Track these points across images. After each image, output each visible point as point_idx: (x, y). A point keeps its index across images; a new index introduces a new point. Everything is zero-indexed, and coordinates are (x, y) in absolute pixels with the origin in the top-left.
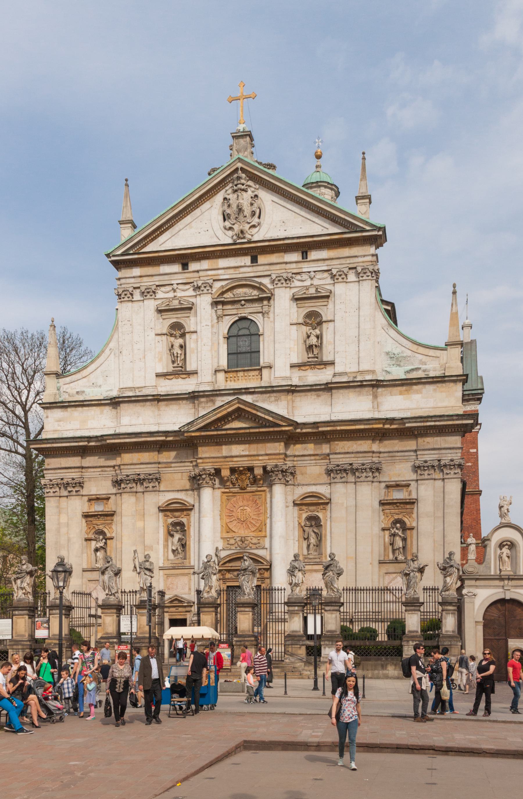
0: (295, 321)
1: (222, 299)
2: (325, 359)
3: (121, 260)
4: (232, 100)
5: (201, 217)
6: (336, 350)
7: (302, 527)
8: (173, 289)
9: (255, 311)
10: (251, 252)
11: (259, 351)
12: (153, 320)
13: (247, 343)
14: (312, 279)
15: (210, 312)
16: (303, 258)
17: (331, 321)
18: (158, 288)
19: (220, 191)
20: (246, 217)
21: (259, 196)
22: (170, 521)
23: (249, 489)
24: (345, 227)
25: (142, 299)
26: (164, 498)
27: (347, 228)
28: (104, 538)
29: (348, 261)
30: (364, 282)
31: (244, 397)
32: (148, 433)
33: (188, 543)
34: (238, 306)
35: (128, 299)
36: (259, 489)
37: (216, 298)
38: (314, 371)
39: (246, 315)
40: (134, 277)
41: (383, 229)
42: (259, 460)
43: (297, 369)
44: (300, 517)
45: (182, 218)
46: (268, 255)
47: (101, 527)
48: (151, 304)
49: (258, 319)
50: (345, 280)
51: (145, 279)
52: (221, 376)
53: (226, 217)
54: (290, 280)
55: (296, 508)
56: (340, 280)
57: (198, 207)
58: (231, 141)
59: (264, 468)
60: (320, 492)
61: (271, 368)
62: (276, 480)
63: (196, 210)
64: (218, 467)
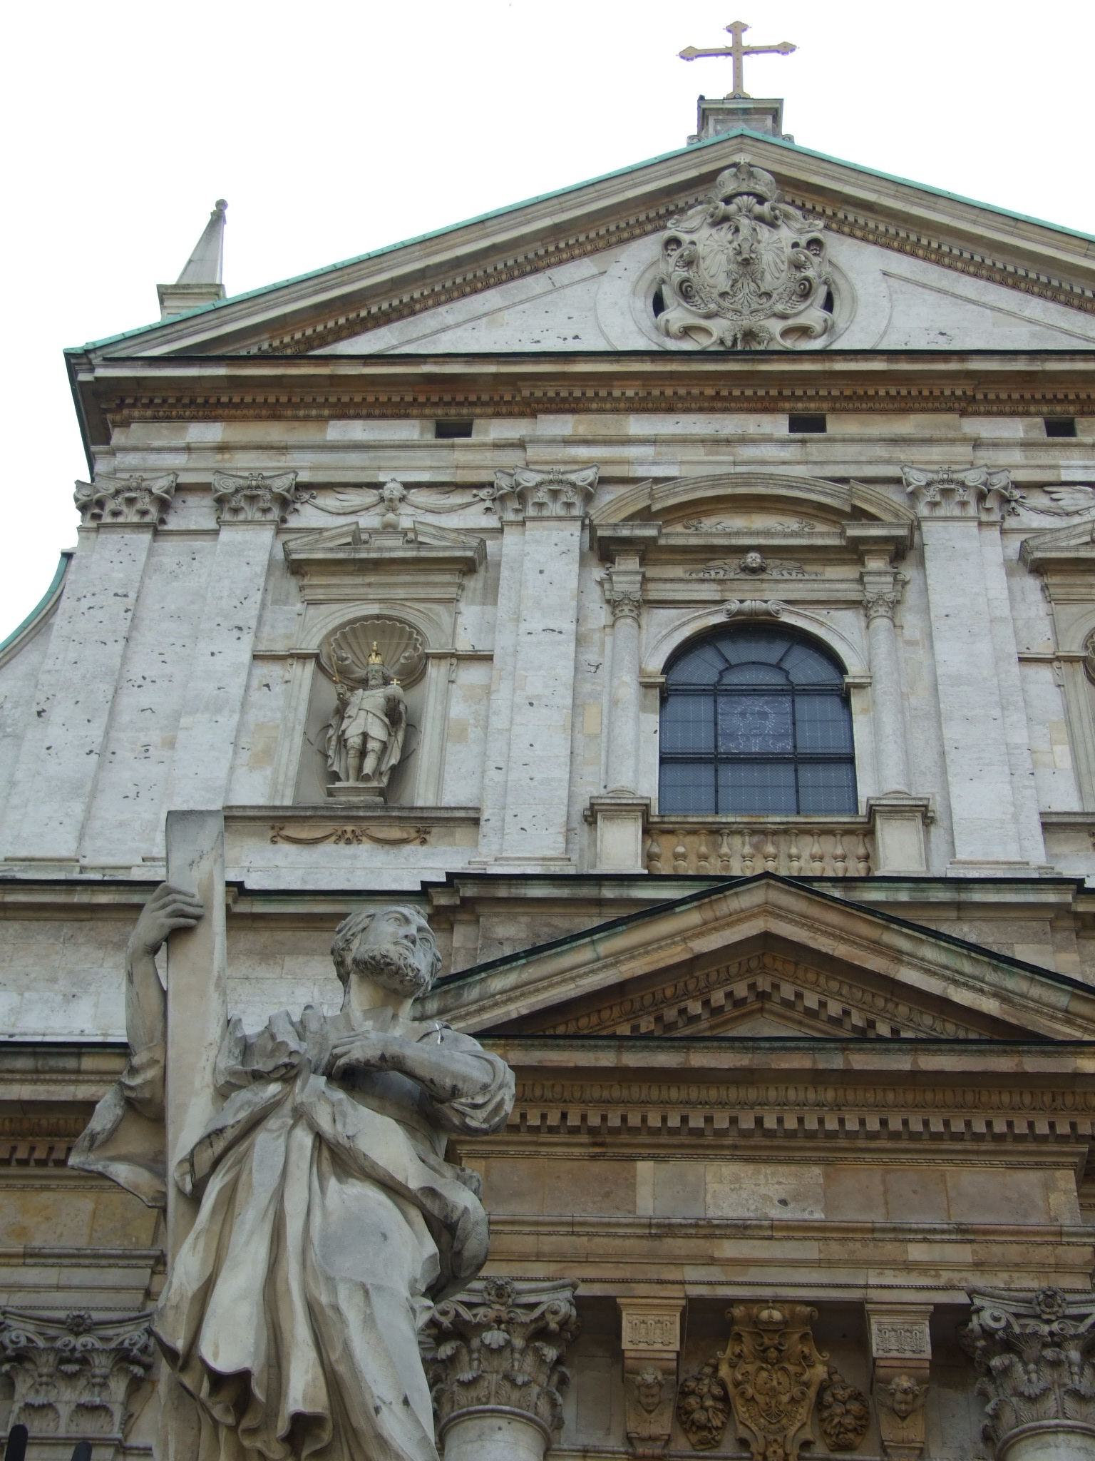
0: (1043, 647)
1: (651, 532)
5: (549, 298)
8: (382, 499)
9: (823, 596)
10: (793, 397)
12: (258, 596)
15: (573, 584)
18: (306, 496)
19: (645, 234)
20: (768, 295)
25: (211, 524)
35: (135, 519)
37: (616, 525)
39: (771, 607)
40: (188, 449)
42: (909, 1267)
46: (878, 418)
57: (536, 270)
61: (927, 819)
62: (1051, 1404)
63: (530, 280)
64: (597, 1290)
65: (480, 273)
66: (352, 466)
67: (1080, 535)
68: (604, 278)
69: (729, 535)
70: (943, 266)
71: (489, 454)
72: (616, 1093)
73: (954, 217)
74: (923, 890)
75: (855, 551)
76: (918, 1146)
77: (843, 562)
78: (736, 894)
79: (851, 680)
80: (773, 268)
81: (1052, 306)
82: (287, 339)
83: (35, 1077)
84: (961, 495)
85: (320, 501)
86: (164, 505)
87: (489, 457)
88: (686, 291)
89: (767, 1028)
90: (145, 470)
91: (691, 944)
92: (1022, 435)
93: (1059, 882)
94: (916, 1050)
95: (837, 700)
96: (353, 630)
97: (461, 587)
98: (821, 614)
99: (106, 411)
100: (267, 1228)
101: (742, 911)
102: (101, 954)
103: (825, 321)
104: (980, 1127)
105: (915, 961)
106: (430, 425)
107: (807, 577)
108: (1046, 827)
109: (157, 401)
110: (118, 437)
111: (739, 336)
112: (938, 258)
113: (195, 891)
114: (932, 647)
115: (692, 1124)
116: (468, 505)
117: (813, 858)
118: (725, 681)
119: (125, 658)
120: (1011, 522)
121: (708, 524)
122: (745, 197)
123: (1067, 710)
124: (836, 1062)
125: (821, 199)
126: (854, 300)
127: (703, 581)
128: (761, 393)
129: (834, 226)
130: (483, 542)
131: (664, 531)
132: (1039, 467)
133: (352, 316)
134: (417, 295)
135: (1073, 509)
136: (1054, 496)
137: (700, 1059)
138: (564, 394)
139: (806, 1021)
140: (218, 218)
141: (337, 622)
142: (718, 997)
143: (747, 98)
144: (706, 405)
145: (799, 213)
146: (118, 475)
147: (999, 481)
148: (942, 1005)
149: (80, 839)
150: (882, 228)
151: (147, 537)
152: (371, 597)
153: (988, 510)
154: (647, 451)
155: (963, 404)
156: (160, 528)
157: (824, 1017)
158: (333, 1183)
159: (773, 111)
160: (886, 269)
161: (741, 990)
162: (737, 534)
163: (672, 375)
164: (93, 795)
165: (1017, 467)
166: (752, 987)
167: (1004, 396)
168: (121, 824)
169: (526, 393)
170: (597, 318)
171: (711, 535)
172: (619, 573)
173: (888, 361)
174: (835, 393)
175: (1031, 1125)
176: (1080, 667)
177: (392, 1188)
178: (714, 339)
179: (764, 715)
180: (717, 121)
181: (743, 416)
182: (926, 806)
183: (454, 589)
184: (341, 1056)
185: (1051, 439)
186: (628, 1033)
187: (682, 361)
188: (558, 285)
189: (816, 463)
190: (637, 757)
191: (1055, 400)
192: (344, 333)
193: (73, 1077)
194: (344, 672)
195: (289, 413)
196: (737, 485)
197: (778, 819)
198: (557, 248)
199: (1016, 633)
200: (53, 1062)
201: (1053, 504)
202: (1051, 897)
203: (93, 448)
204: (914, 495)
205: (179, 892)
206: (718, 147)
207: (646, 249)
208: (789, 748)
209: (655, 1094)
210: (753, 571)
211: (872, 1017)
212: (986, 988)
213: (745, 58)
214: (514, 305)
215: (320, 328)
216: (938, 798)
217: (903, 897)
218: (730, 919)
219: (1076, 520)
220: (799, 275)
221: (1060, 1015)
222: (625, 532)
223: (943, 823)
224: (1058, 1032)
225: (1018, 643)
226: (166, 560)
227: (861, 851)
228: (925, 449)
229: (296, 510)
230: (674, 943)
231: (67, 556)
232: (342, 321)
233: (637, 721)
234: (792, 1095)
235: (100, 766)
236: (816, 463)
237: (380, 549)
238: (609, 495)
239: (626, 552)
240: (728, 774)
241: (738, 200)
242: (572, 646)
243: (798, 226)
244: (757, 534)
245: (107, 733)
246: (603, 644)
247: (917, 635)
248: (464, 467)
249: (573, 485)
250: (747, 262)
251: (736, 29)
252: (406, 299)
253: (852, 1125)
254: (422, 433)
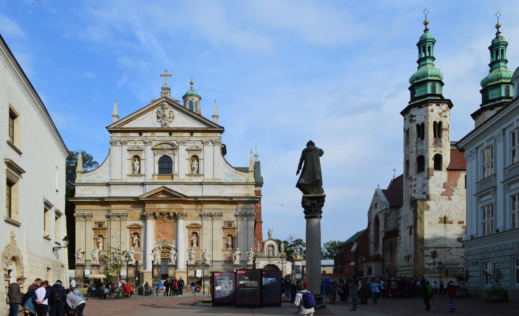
4: (161, 76)
7: (190, 236)
11: (172, 168)
13: (167, 165)
16: (191, 135)
18: (129, 141)
21: (173, 111)
22: (132, 232)
23: (167, 221)
24: (208, 126)
26: (130, 223)
27: (209, 126)
28: (102, 238)
29: (209, 138)
31: (165, 186)
33: (140, 241)
34: (163, 151)
36: (172, 221)
41: (223, 128)
43: (188, 176)
44: (189, 232)
45: (140, 116)
47: (101, 234)
48: (125, 148)
49: (172, 156)
50: (208, 145)
51: (123, 138)
52: (155, 177)
53: (158, 118)
54: (185, 143)
55: (188, 229)
56: (206, 145)
58: (161, 90)
59: (174, 213)
60: (198, 223)
75: (173, 149)
106: (139, 134)
154: (157, 138)
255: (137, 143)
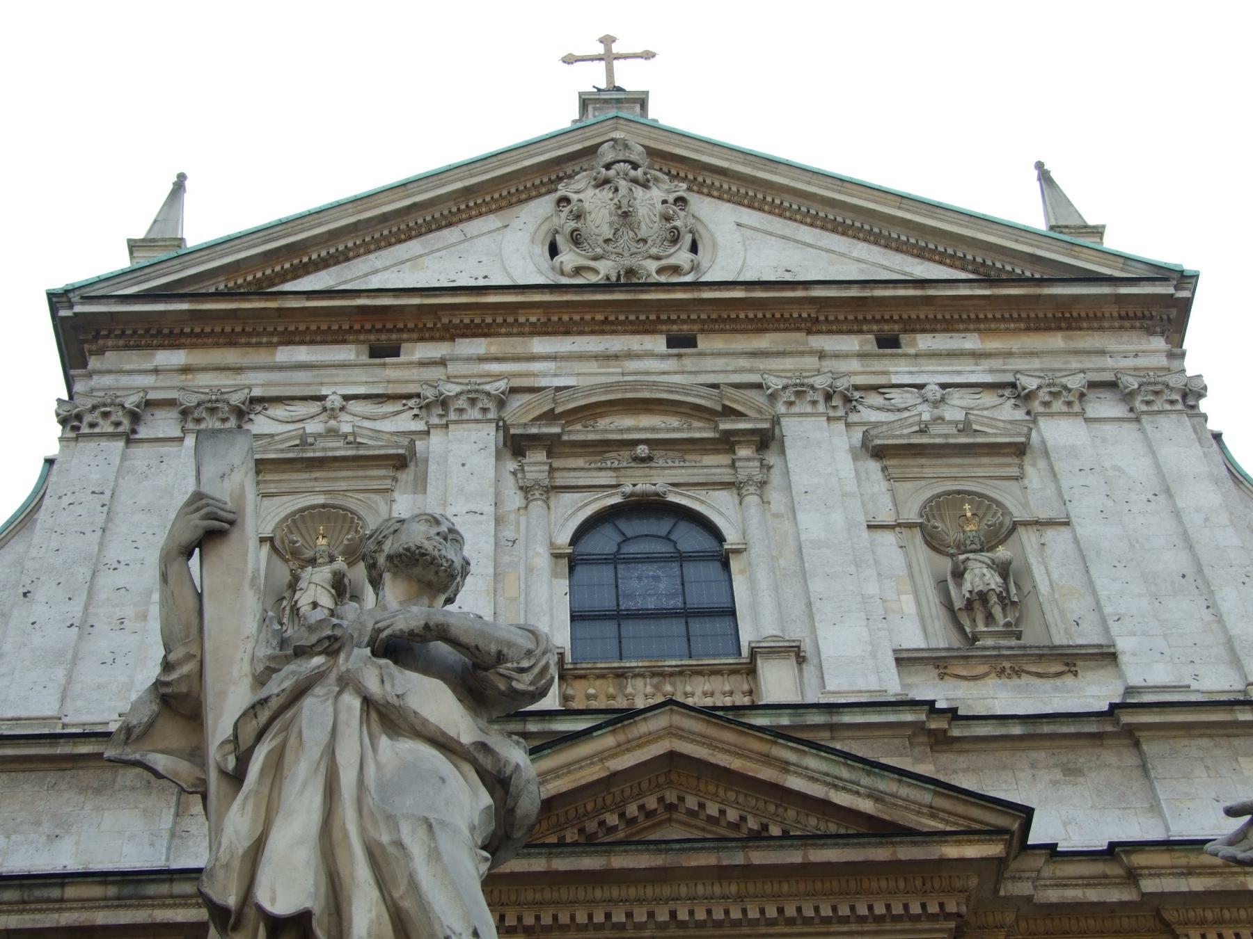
0: (886, 516)
1: (555, 430)
2: (1059, 640)
3: (112, 315)
5: (462, 246)
6: (1108, 610)
8: (325, 409)
9: (702, 479)
14: (936, 404)
17: (1051, 523)
18: (259, 408)
19: (540, 195)
20: (644, 241)
25: (178, 433)
30: (1164, 421)
32: (104, 877)
35: (110, 429)
37: (526, 424)
38: (1016, 681)
39: (659, 489)
40: (156, 371)
46: (739, 336)
57: (450, 225)
61: (801, 659)
63: (445, 232)
65: (403, 227)
66: (299, 382)
67: (911, 425)
68: (508, 229)
69: (621, 431)
70: (785, 218)
71: (415, 371)
72: (548, 895)
73: (793, 179)
74: (801, 715)
75: (727, 442)
76: (812, 930)
77: (717, 452)
78: (645, 719)
79: (729, 547)
80: (647, 220)
81: (874, 248)
82: (240, 281)
83: (21, 907)
84: (811, 395)
85: (271, 412)
86: (135, 417)
87: (416, 373)
88: (576, 239)
89: (673, 833)
90: (118, 389)
91: (607, 764)
92: (858, 348)
93: (913, 704)
94: (806, 845)
95: (718, 564)
96: (302, 517)
97: (395, 479)
98: (701, 494)
99: (84, 341)
100: (320, 781)
101: (650, 734)
102: (82, 798)
103: (692, 261)
104: (863, 910)
105: (800, 770)
106: (365, 349)
107: (687, 464)
108: (897, 660)
109: (129, 332)
110: (94, 363)
111: (622, 273)
112: (780, 212)
113: (227, 499)
114: (795, 518)
115: (615, 919)
116: (399, 413)
117: (705, 694)
118: (622, 551)
119: (101, 546)
120: (853, 417)
121: (602, 423)
122: (622, 164)
123: (910, 566)
124: (738, 859)
125: (683, 167)
126: (715, 245)
127: (601, 469)
128: (642, 317)
129: (695, 188)
130: (413, 442)
131: (567, 429)
132: (873, 373)
133: (296, 261)
134: (350, 244)
135: (903, 406)
136: (887, 396)
137: (620, 861)
138: (477, 321)
139: (709, 827)
140: (179, 186)
141: (289, 511)
142: (632, 810)
143: (620, 89)
144: (597, 328)
145: (666, 178)
146: (94, 394)
147: (842, 384)
148: (825, 807)
149: (62, 700)
150: (734, 189)
151: (120, 444)
152: (317, 489)
153: (834, 407)
155: (809, 325)
156: (132, 437)
157: (724, 823)
158: (384, 741)
159: (641, 101)
160: (739, 221)
161: (651, 803)
162: (628, 430)
163: (567, 304)
164: (74, 662)
165: (855, 373)
166: (661, 800)
167: (841, 317)
168: (99, 687)
169: (445, 320)
170: (502, 260)
171: (606, 431)
172: (530, 464)
173: (746, 290)
174: (704, 316)
175: (906, 907)
176: (917, 531)
177: (445, 744)
178: (600, 276)
179: (656, 578)
180: (595, 109)
181: (628, 337)
182: (799, 647)
183: (389, 481)
184: (385, 629)
185: (882, 351)
186: (556, 841)
187: (576, 293)
188: (469, 236)
189: (690, 373)
190: (551, 614)
191: (883, 320)
192: (289, 277)
193: (57, 906)
194: (295, 553)
195: (243, 340)
196: (626, 391)
197: (674, 663)
198: (467, 206)
199: (863, 504)
200: (38, 893)
201: (887, 402)
202: (908, 717)
203: (73, 372)
204: (773, 397)
205: (213, 499)
206: (598, 126)
207: (542, 207)
208: (680, 605)
209: (581, 894)
210: (643, 460)
211: (765, 821)
212: (862, 790)
213: (615, 62)
214: (432, 252)
215: (268, 272)
216: (808, 641)
217: (785, 721)
218: (640, 741)
219: (906, 414)
220: (668, 226)
221: (925, 810)
222: (534, 430)
223: (813, 661)
224: (925, 825)
225: (866, 513)
226: (137, 463)
227: (746, 687)
228: (779, 360)
229: (251, 420)
230: (592, 763)
231: (50, 462)
232: (287, 266)
233: (550, 585)
234: (700, 889)
235: (80, 638)
236: (690, 373)
237: (324, 449)
238: (517, 402)
239: (535, 447)
240: (629, 628)
241: (616, 166)
242: (492, 524)
243: (666, 187)
244: (645, 430)
245: (86, 609)
246: (518, 523)
247: (782, 509)
248: (394, 382)
249: (488, 394)
250: (626, 215)
251: (607, 41)
252: (341, 248)
253: (753, 914)
254: (357, 355)
255: (344, 417)
